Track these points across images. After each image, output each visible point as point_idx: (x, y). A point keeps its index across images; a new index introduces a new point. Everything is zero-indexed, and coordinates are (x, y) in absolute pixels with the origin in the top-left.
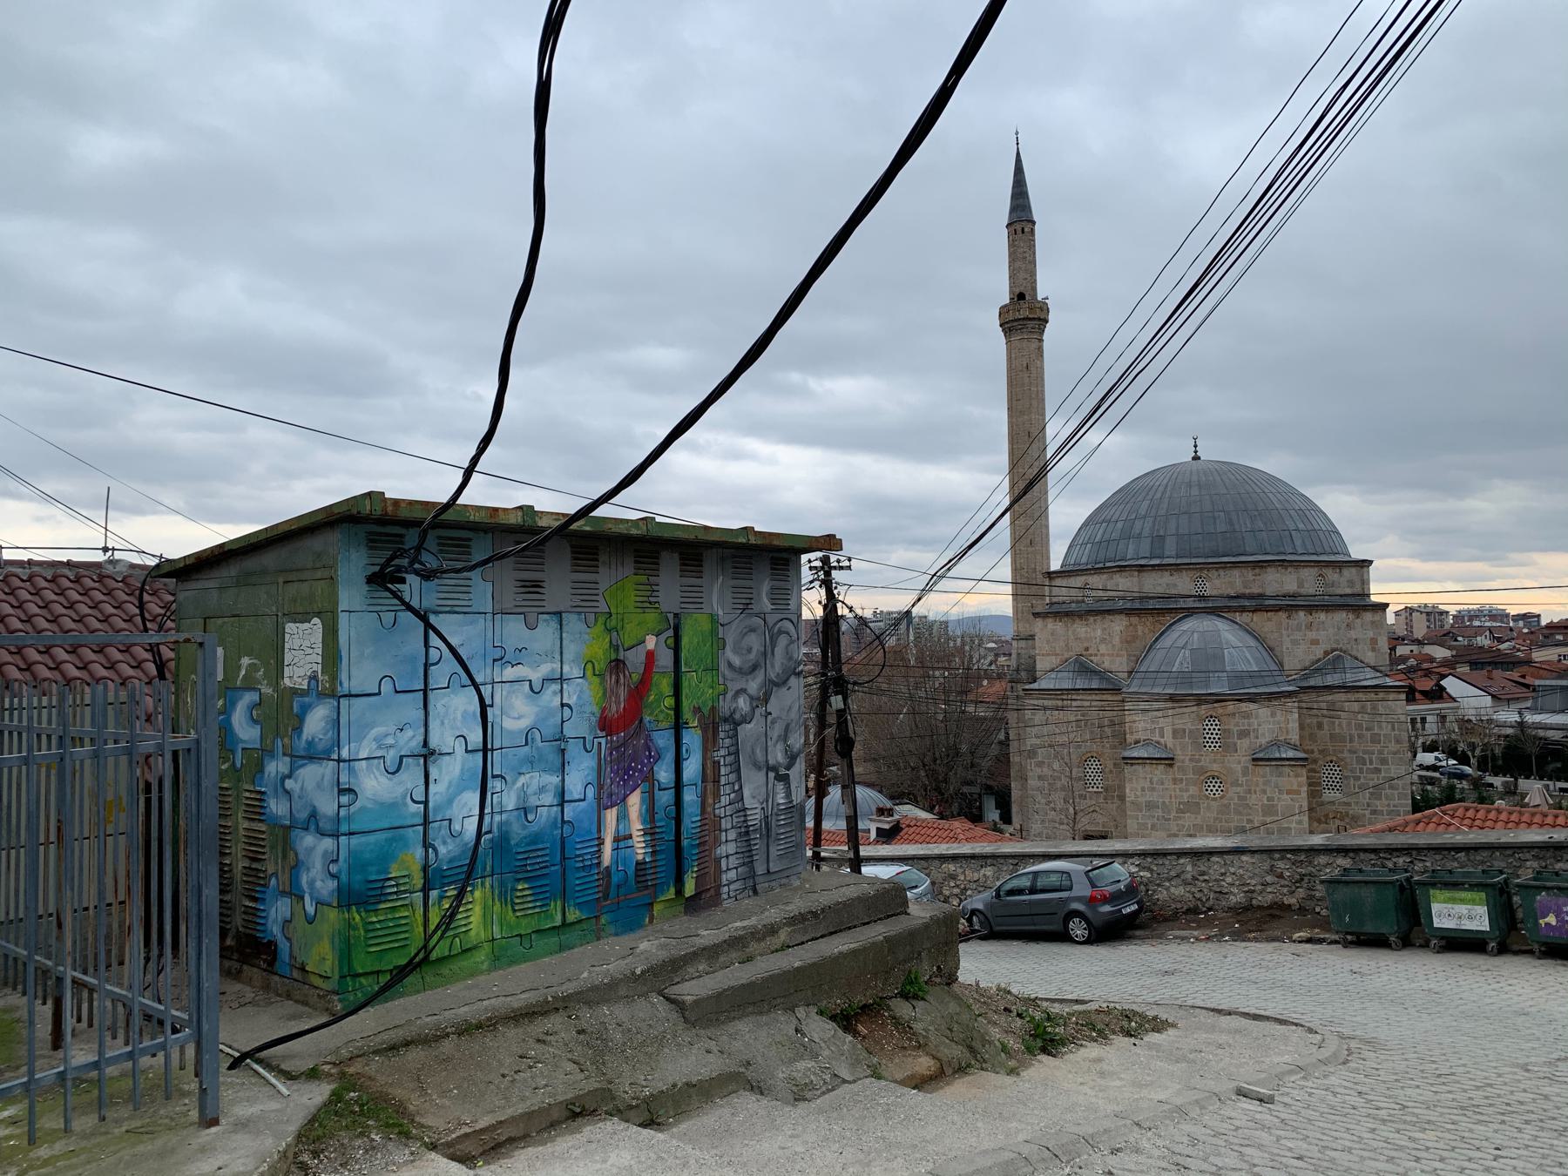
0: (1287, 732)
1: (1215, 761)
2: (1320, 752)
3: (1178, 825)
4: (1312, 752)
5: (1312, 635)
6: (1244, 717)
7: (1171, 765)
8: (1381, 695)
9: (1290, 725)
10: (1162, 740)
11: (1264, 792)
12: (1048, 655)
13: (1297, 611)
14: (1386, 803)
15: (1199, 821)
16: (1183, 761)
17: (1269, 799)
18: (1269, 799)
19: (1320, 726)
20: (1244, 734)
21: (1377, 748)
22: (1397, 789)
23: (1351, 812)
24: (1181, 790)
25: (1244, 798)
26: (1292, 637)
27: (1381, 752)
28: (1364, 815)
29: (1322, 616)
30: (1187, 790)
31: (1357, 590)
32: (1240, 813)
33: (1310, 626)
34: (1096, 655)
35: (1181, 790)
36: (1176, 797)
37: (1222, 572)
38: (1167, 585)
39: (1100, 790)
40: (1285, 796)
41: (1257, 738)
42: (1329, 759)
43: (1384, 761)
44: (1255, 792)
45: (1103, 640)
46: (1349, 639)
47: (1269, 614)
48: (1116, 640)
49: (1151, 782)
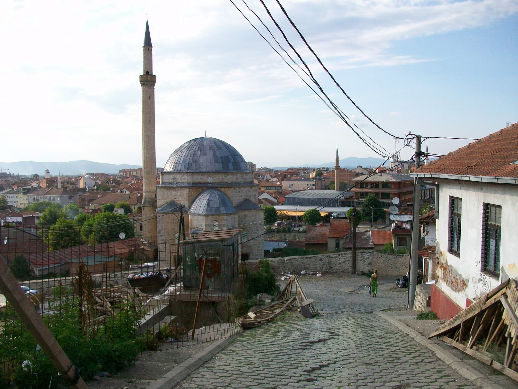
5: (240, 194)
10: (202, 228)
12: (161, 200)
33: (239, 192)
34: (178, 200)
37: (216, 175)
43: (258, 230)
48: (185, 196)
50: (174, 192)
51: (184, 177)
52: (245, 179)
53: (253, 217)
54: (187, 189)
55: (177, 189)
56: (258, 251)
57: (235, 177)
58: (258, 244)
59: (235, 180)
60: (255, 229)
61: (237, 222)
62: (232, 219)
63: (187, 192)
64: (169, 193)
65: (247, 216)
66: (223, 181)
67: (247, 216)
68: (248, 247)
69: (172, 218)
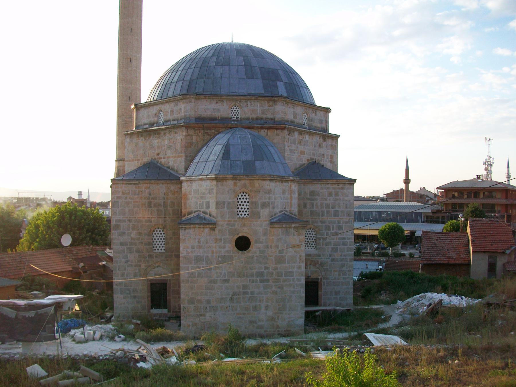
1: (244, 225)
5: (301, 148)
6: (266, 193)
9: (293, 201)
10: (208, 211)
11: (277, 247)
12: (133, 160)
20: (264, 205)
22: (346, 245)
24: (220, 247)
26: (290, 148)
27: (339, 222)
29: (307, 137)
31: (324, 125)
34: (164, 158)
35: (220, 247)
37: (249, 103)
38: (214, 109)
39: (163, 251)
40: (291, 249)
43: (340, 228)
44: (271, 247)
45: (169, 147)
46: (320, 154)
48: (179, 146)
50: (157, 141)
51: (178, 108)
52: (311, 120)
53: (331, 198)
54: (184, 129)
55: (162, 133)
56: (339, 275)
57: (292, 110)
58: (342, 260)
59: (290, 117)
60: (335, 225)
61: (295, 202)
62: (284, 192)
63: (183, 137)
64: (147, 144)
65: (318, 195)
66: (264, 116)
67: (318, 195)
68: (317, 266)
69: (147, 195)
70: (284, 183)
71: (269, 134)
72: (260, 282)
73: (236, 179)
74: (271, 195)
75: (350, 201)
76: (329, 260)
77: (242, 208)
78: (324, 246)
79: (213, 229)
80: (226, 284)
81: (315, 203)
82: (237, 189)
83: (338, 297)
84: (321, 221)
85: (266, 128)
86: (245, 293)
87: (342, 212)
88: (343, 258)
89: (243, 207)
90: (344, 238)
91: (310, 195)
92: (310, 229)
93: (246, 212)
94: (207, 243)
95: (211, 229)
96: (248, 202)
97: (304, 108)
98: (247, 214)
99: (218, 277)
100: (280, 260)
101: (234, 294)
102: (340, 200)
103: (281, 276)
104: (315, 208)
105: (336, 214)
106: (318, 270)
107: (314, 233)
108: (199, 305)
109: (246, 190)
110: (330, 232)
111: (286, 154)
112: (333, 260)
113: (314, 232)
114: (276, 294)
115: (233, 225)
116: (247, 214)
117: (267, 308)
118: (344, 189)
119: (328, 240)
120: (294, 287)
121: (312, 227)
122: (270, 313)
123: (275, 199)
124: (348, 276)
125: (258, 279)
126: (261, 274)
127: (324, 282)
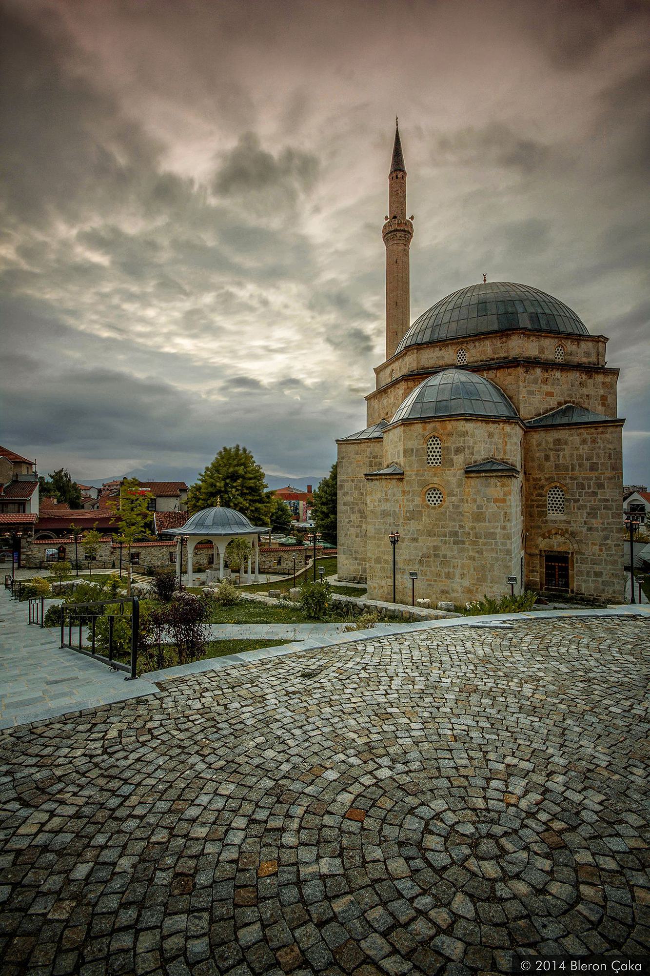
0: (505, 453)
2: (547, 479)
3: (404, 530)
4: (540, 480)
6: (460, 436)
7: (401, 480)
8: (600, 430)
11: (475, 501)
13: (534, 368)
14: (601, 521)
15: (420, 527)
16: (410, 476)
17: (479, 507)
18: (479, 507)
19: (547, 458)
20: (458, 451)
21: (594, 474)
23: (570, 529)
25: (458, 507)
27: (598, 478)
28: (581, 532)
29: (558, 374)
30: (413, 501)
32: (454, 520)
33: (545, 381)
36: (404, 507)
37: (477, 344)
41: (473, 454)
42: (553, 485)
43: (601, 486)
44: (467, 501)
47: (510, 370)
49: (386, 495)
51: (404, 363)
53: (586, 447)
56: (601, 550)
62: (490, 435)
66: (496, 356)
67: (566, 443)
68: (567, 536)
70: (491, 425)
71: (498, 375)
72: (454, 544)
73: (425, 423)
74: (466, 438)
75: (615, 449)
76: (584, 530)
77: (433, 456)
78: (576, 511)
79: (401, 480)
80: (415, 544)
81: (561, 455)
82: (427, 433)
83: (600, 580)
84: (571, 478)
85: (494, 369)
86: (436, 556)
87: (603, 464)
88: (606, 528)
89: (434, 454)
90: (608, 500)
91: (554, 445)
92: (556, 488)
93: (438, 459)
94: (394, 496)
95: (398, 479)
96: (440, 448)
97: (556, 340)
98: (438, 462)
99: (406, 535)
100: (479, 517)
101: (424, 556)
102: (599, 448)
103: (481, 538)
104: (561, 462)
105: (594, 467)
106: (568, 541)
107: (561, 494)
108: (386, 566)
109: (436, 435)
110: (584, 491)
111: (521, 396)
112: (590, 529)
113: (561, 491)
114: (474, 560)
115: (423, 476)
116: (438, 462)
117: (462, 576)
118: (607, 433)
119: (581, 502)
120: (497, 552)
121: (558, 485)
122: (466, 583)
123: (475, 443)
124: (614, 552)
125: (452, 540)
126: (456, 534)
127: (577, 558)
